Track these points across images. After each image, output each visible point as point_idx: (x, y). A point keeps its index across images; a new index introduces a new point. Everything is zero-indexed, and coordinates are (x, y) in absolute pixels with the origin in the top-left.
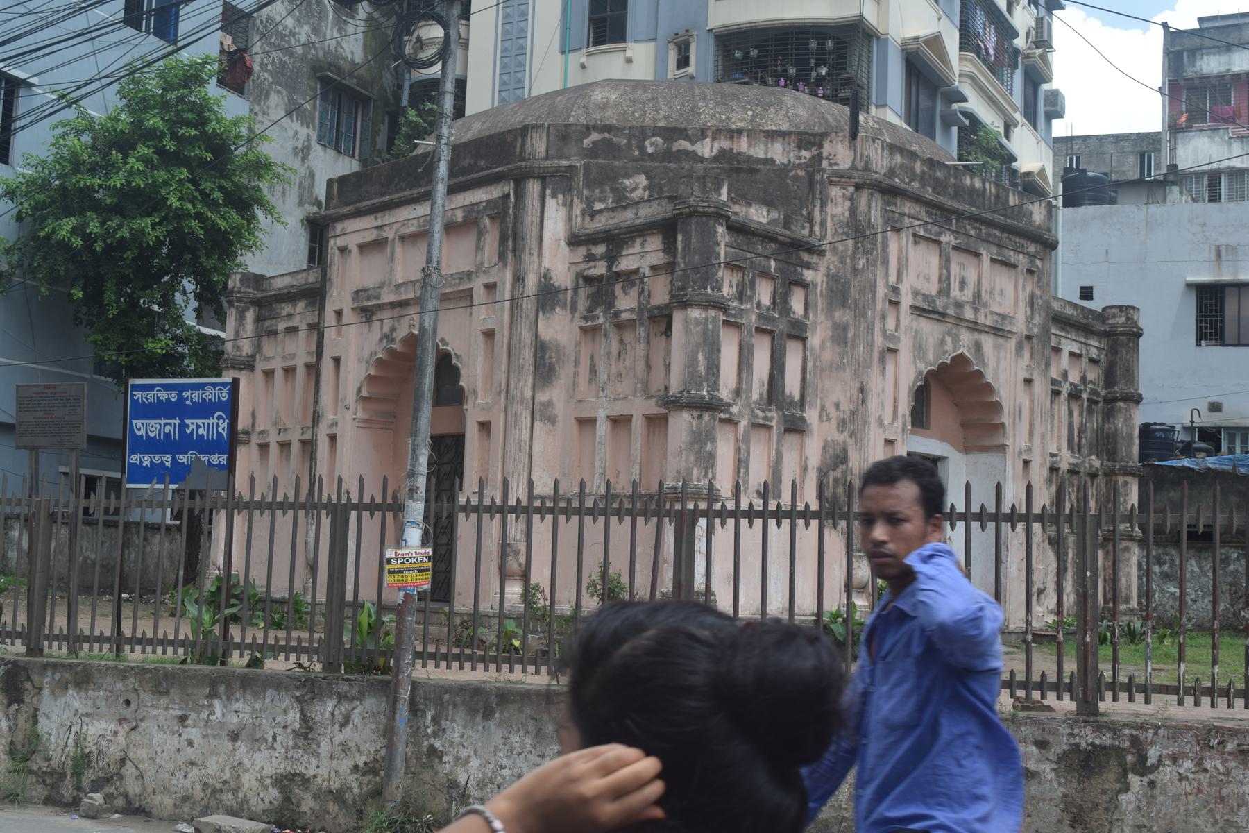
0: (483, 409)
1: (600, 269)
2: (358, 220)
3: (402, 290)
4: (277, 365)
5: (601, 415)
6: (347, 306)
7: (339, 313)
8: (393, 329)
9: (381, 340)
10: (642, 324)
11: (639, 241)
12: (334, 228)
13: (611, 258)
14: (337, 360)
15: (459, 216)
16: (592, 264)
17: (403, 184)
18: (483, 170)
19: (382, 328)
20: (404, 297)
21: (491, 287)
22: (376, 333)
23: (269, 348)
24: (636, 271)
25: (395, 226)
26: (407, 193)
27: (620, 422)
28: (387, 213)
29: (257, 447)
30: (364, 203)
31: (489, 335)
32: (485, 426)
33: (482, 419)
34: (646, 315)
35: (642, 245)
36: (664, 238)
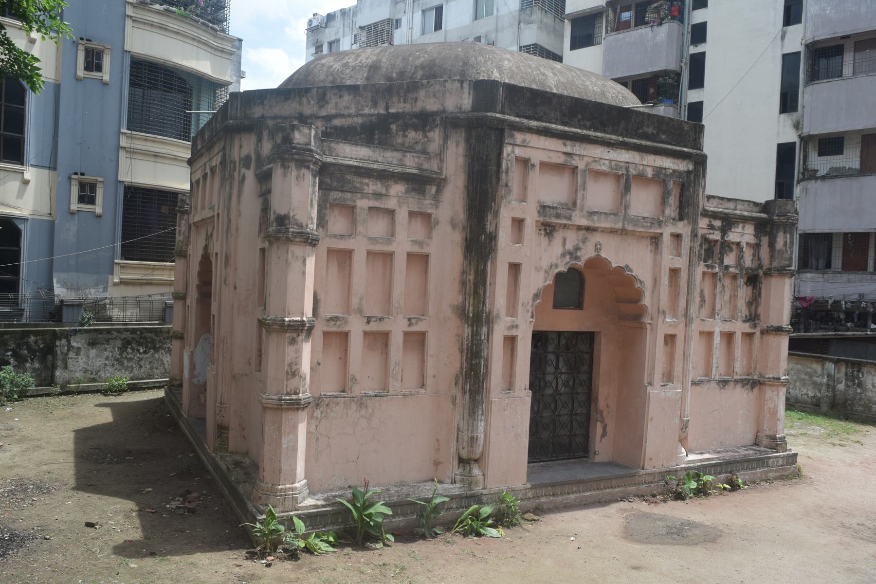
0: (670, 325)
1: (716, 236)
2: (543, 138)
3: (596, 218)
4: (359, 246)
5: (717, 330)
6: (531, 219)
7: (519, 223)
8: (577, 249)
9: (563, 255)
10: (742, 277)
11: (741, 225)
12: (512, 136)
13: (724, 231)
14: (515, 268)
15: (650, 173)
16: (711, 231)
17: (588, 123)
18: (663, 142)
19: (564, 244)
20: (597, 225)
21: (677, 237)
22: (557, 248)
23: (338, 223)
24: (738, 244)
25: (586, 159)
26: (591, 133)
27: (729, 337)
28: (577, 144)
29: (322, 335)
30: (553, 126)
31: (674, 273)
32: (670, 339)
33: (669, 333)
34: (744, 272)
35: (743, 228)
36: (757, 228)
